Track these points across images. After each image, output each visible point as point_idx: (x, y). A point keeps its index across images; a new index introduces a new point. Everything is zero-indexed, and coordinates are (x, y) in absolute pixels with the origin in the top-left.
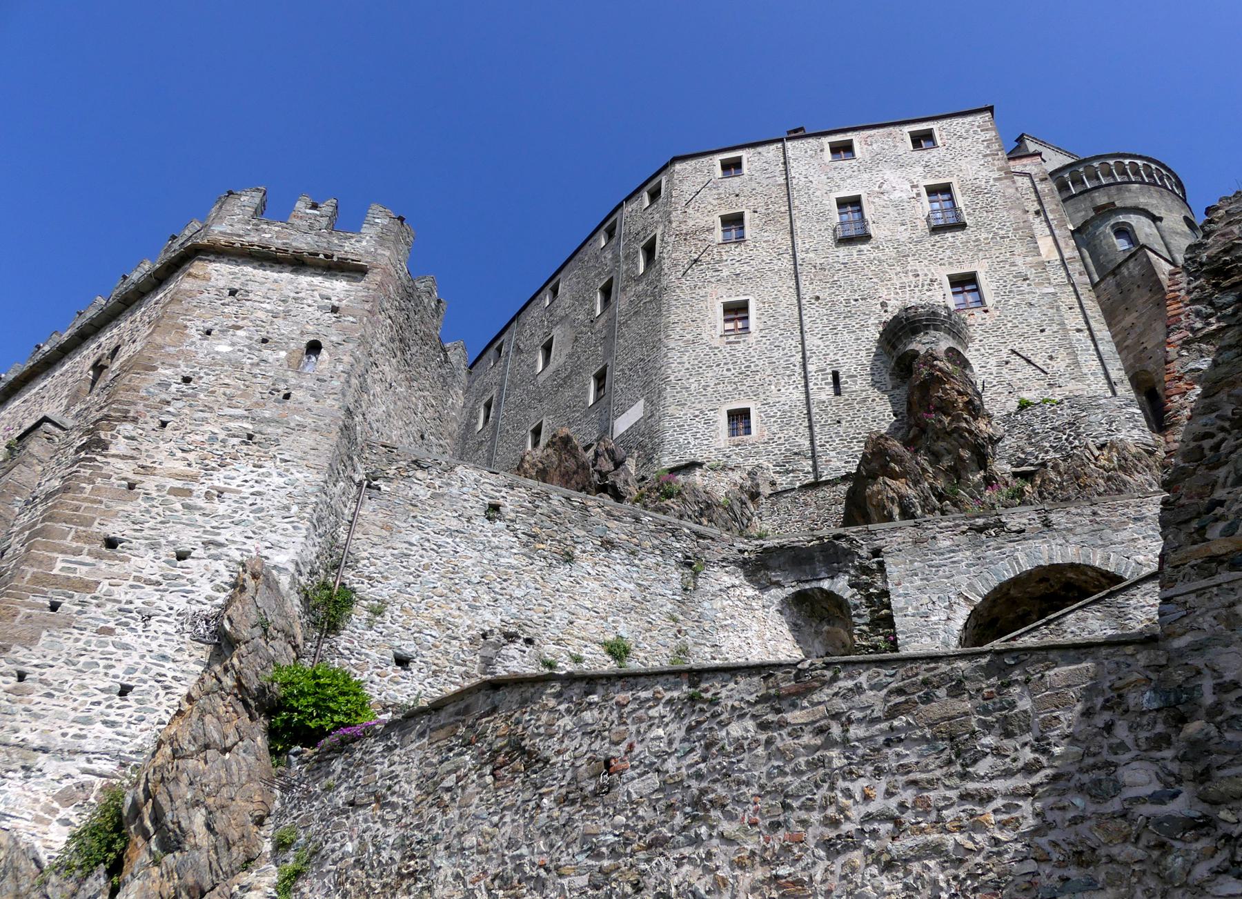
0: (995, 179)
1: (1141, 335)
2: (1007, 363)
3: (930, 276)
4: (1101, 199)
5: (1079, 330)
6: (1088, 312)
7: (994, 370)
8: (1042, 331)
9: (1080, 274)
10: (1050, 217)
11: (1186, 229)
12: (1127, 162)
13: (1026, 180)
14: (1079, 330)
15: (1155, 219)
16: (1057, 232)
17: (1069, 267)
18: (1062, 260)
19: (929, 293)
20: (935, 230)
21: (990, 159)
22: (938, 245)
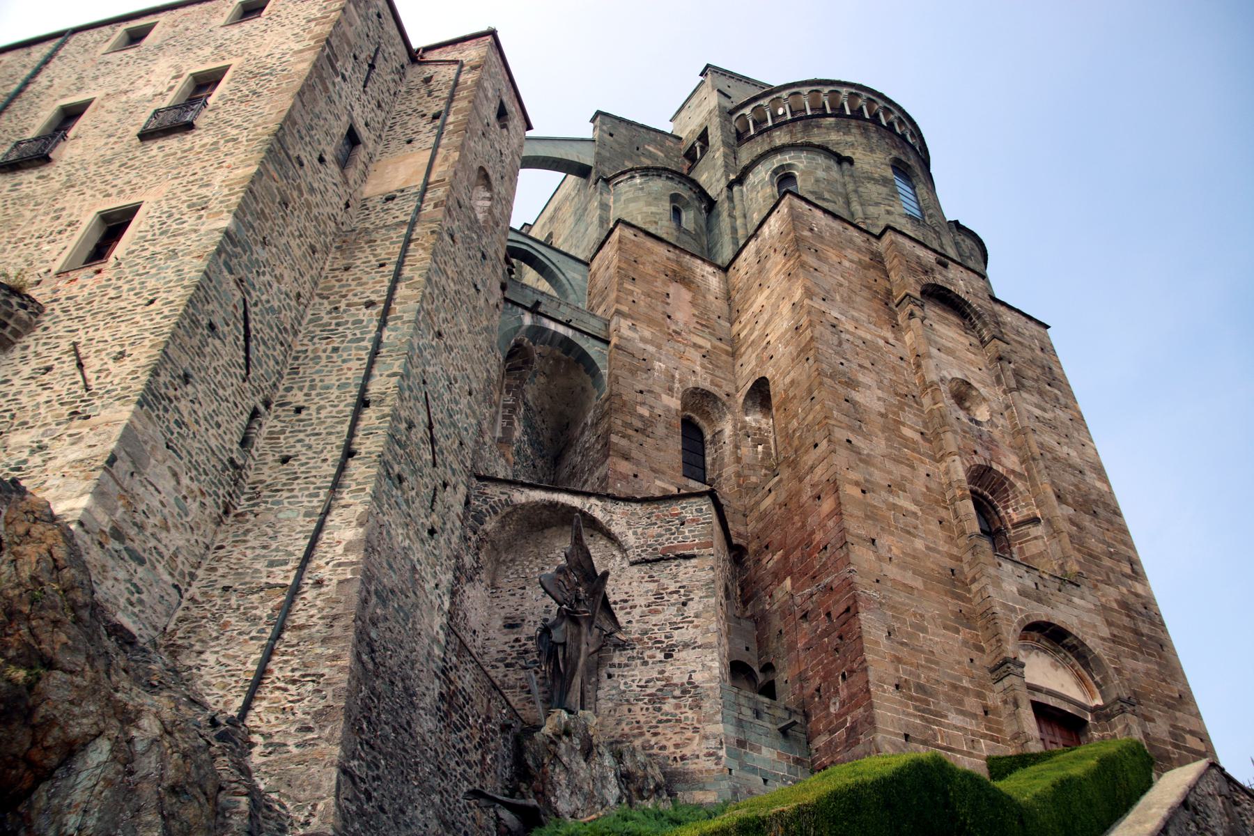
0: (296, 53)
1: (767, 324)
2: (49, 369)
3: (73, 218)
4: (780, 138)
5: (370, 304)
6: (406, 272)
7: (14, 390)
8: (152, 302)
9: (436, 206)
10: (451, 119)
11: (889, 173)
12: (826, 90)
13: (452, 71)
14: (370, 304)
15: (841, 160)
16: (444, 141)
17: (428, 195)
18: (426, 183)
19: (46, 247)
20: (146, 136)
21: (313, 24)
22: (130, 163)
